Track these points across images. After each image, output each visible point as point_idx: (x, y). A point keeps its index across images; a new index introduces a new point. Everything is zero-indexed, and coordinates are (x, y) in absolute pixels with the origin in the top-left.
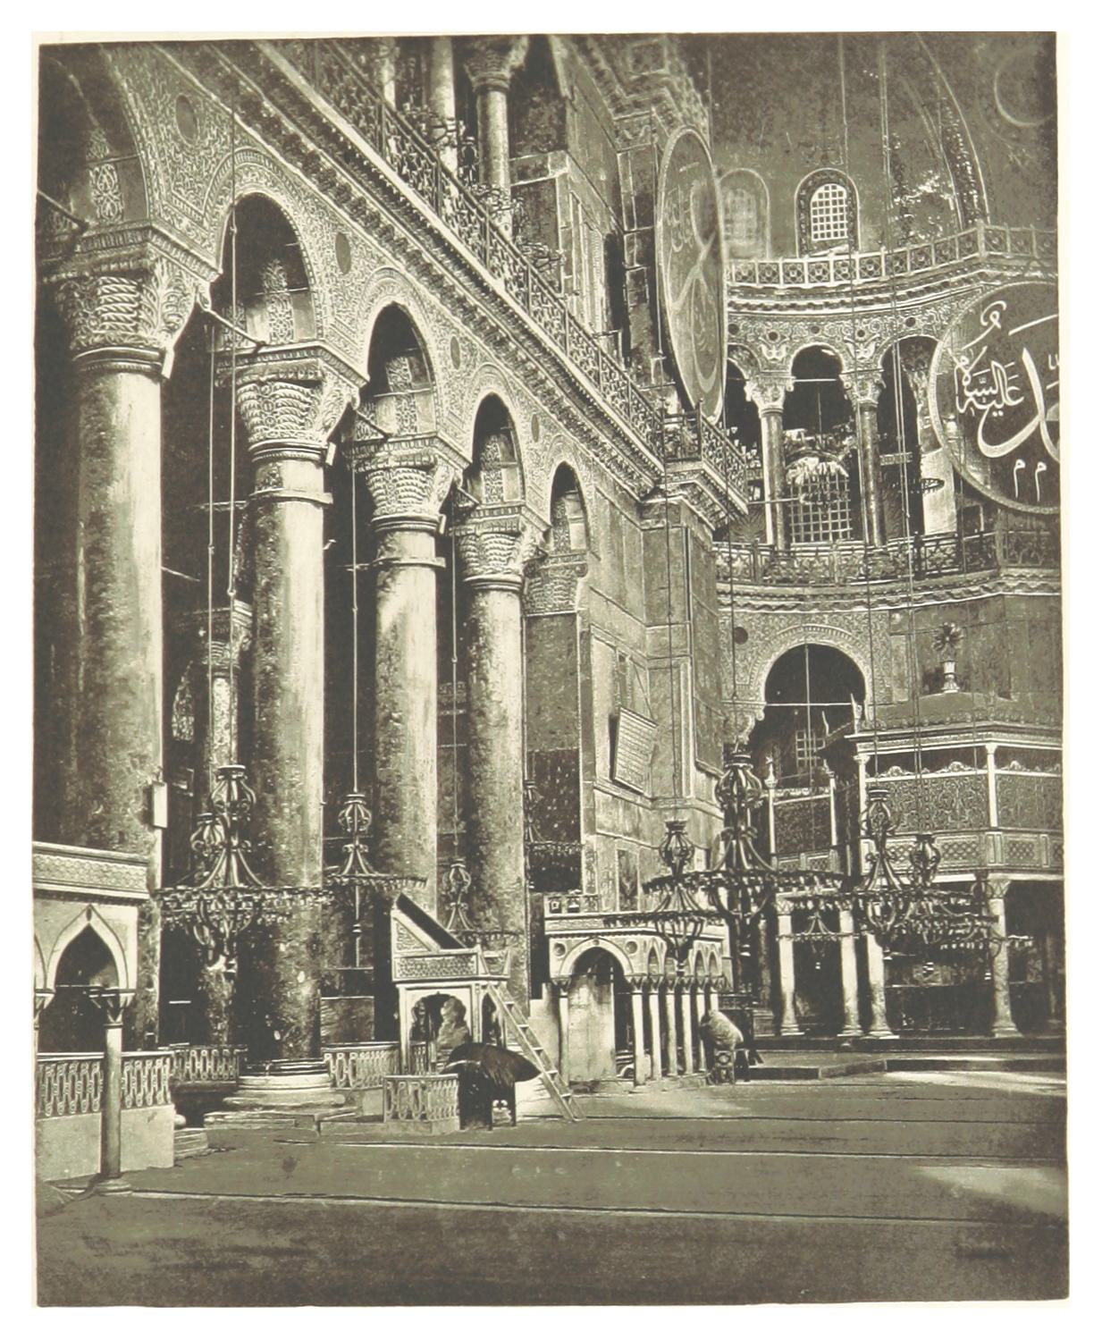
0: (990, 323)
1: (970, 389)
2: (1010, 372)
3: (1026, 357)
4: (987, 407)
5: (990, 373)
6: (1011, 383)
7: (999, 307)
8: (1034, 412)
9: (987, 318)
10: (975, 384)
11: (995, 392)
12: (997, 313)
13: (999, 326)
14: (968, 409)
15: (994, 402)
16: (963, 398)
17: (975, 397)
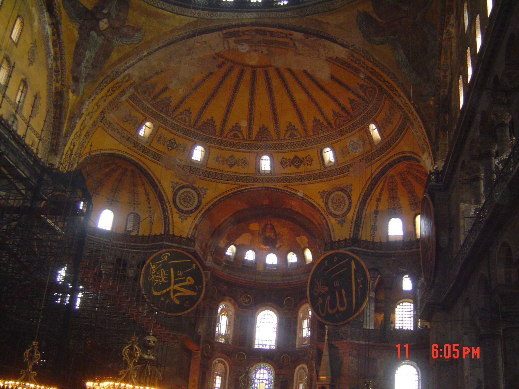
0: (164, 259)
1: (154, 275)
2: (166, 273)
3: (172, 269)
4: (157, 281)
5: (161, 272)
6: (166, 276)
7: (167, 255)
8: (170, 285)
9: (163, 257)
10: (155, 274)
11: (161, 277)
12: (166, 256)
13: (166, 260)
14: (151, 280)
15: (159, 280)
16: (151, 277)
17: (155, 277)
